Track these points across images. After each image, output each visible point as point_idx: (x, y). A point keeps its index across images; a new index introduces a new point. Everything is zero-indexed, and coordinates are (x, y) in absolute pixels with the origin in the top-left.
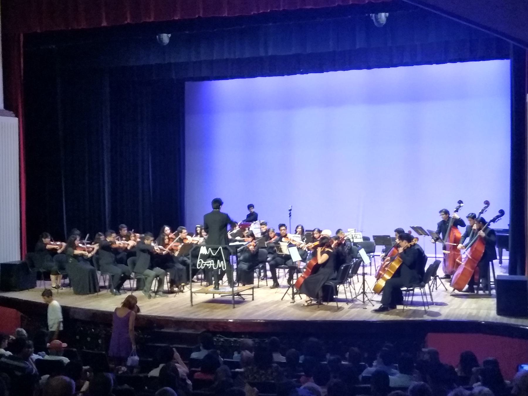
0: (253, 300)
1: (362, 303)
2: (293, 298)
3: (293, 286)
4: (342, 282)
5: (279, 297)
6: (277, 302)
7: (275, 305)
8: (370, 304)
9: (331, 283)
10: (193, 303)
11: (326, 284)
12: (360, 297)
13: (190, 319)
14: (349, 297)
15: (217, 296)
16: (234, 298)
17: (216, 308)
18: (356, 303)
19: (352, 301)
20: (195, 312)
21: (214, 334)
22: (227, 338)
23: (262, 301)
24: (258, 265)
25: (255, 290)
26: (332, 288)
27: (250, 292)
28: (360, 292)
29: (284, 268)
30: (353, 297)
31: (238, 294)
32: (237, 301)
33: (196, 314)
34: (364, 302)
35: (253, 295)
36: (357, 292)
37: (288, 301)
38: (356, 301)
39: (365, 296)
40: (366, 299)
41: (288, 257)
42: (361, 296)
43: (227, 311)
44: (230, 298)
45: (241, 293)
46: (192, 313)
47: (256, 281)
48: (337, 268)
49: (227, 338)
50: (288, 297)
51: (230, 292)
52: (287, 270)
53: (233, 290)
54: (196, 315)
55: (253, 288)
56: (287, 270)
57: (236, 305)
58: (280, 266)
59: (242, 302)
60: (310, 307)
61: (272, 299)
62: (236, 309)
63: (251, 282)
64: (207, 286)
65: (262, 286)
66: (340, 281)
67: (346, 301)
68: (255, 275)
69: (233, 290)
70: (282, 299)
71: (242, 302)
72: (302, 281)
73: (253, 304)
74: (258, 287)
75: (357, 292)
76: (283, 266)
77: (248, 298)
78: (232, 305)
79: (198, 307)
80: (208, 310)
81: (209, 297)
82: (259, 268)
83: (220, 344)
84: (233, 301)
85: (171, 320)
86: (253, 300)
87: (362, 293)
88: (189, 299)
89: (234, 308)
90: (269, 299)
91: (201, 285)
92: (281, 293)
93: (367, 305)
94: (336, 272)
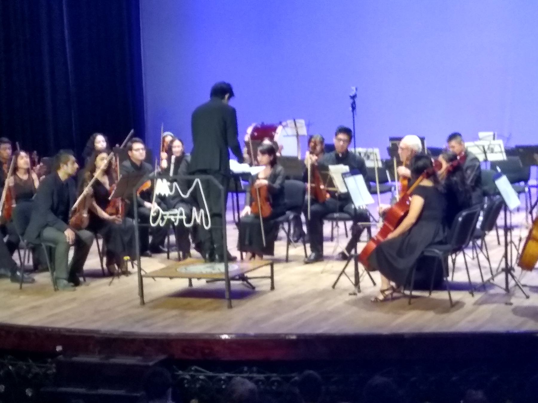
0: (273, 288)
1: (503, 292)
2: (357, 283)
3: (358, 258)
4: (459, 248)
5: (328, 281)
6: (322, 293)
7: (318, 300)
8: (519, 293)
9: (437, 251)
10: (146, 299)
11: (427, 254)
12: (500, 279)
13: (132, 333)
14: (476, 277)
15: (198, 284)
16: (229, 285)
17: (194, 309)
18: (492, 291)
19: (484, 287)
20: (145, 319)
21: (184, 365)
22: (211, 374)
23: (292, 291)
24: (283, 214)
25: (276, 267)
26: (440, 261)
27: (266, 270)
28: (500, 270)
29: (345, 220)
30: (487, 277)
31: (242, 278)
32: (237, 292)
33: (149, 322)
34: (507, 289)
35: (272, 277)
36: (494, 266)
37: (345, 290)
38: (492, 286)
39: (510, 277)
40: (512, 283)
41: (346, 198)
42: (502, 276)
43: (216, 314)
44: (221, 285)
45: (248, 275)
46: (138, 322)
47: (280, 248)
48: (448, 219)
49: (211, 374)
50: (347, 282)
51: (221, 274)
52: (350, 224)
53: (227, 267)
54: (147, 326)
55: (272, 265)
56: (350, 224)
57: (234, 302)
58: (330, 216)
59: (248, 293)
60: (390, 304)
61: (314, 288)
62: (235, 310)
63: (270, 250)
64: (179, 259)
65: (296, 259)
66: (456, 247)
67: (469, 287)
68: (282, 233)
69: (227, 267)
70: (334, 286)
71: (248, 293)
72: (373, 246)
73: (273, 297)
74: (287, 260)
75: (494, 266)
76: (336, 215)
77: (264, 285)
78: (225, 302)
79: (155, 307)
80: (174, 312)
81: (181, 284)
82: (288, 221)
83: (198, 386)
84: (227, 294)
85: (92, 338)
86: (273, 288)
87: (503, 270)
88: (137, 290)
89: (230, 307)
90: (306, 288)
91: (168, 258)
92: (334, 273)
93: (513, 295)
94: (447, 229)
